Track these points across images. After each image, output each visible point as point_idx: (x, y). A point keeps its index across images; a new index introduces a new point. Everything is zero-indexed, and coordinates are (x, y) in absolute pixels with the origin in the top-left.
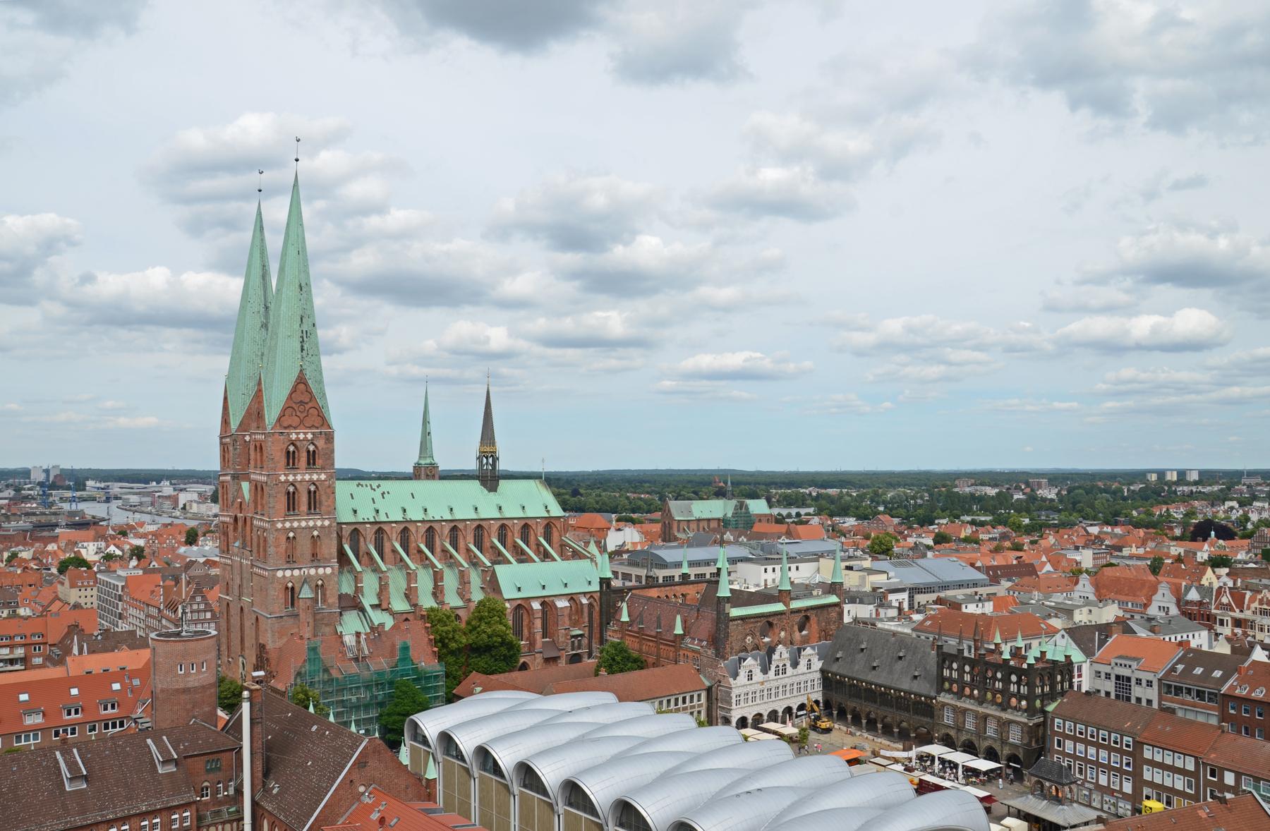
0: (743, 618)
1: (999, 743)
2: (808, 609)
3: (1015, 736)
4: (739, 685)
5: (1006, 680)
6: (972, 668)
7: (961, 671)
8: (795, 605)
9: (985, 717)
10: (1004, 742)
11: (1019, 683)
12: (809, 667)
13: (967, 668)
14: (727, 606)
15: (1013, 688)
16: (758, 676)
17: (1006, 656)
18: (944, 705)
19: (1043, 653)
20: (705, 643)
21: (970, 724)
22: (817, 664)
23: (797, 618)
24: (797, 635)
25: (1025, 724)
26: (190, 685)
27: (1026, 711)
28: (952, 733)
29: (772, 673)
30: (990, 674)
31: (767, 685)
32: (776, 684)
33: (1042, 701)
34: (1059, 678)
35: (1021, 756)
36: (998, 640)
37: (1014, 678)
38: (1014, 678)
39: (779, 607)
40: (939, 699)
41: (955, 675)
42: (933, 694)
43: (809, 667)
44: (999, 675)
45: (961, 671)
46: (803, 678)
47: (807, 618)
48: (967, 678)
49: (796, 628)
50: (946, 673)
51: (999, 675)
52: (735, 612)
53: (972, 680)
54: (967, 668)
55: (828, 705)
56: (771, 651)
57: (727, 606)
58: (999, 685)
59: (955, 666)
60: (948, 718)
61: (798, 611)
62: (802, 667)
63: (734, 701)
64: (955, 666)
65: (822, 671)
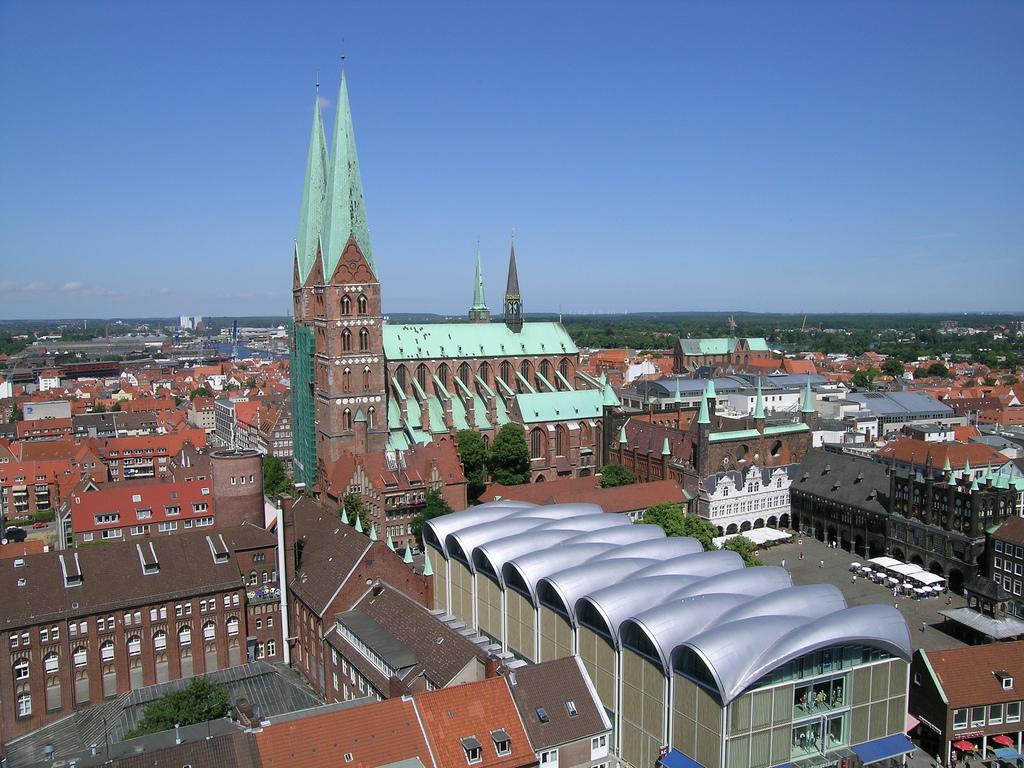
0: (719, 442)
2: (780, 435)
4: (716, 498)
8: (769, 431)
12: (779, 485)
14: (707, 431)
16: (733, 492)
17: (953, 482)
22: (787, 483)
23: (771, 443)
24: (770, 456)
26: (241, 494)
28: (902, 548)
29: (745, 489)
31: (741, 500)
32: (749, 499)
33: (984, 524)
34: (1002, 504)
36: (948, 467)
39: (754, 433)
43: (779, 485)
47: (779, 444)
52: (713, 437)
55: (794, 516)
56: (746, 470)
57: (707, 431)
61: (771, 436)
62: (773, 486)
63: (711, 510)
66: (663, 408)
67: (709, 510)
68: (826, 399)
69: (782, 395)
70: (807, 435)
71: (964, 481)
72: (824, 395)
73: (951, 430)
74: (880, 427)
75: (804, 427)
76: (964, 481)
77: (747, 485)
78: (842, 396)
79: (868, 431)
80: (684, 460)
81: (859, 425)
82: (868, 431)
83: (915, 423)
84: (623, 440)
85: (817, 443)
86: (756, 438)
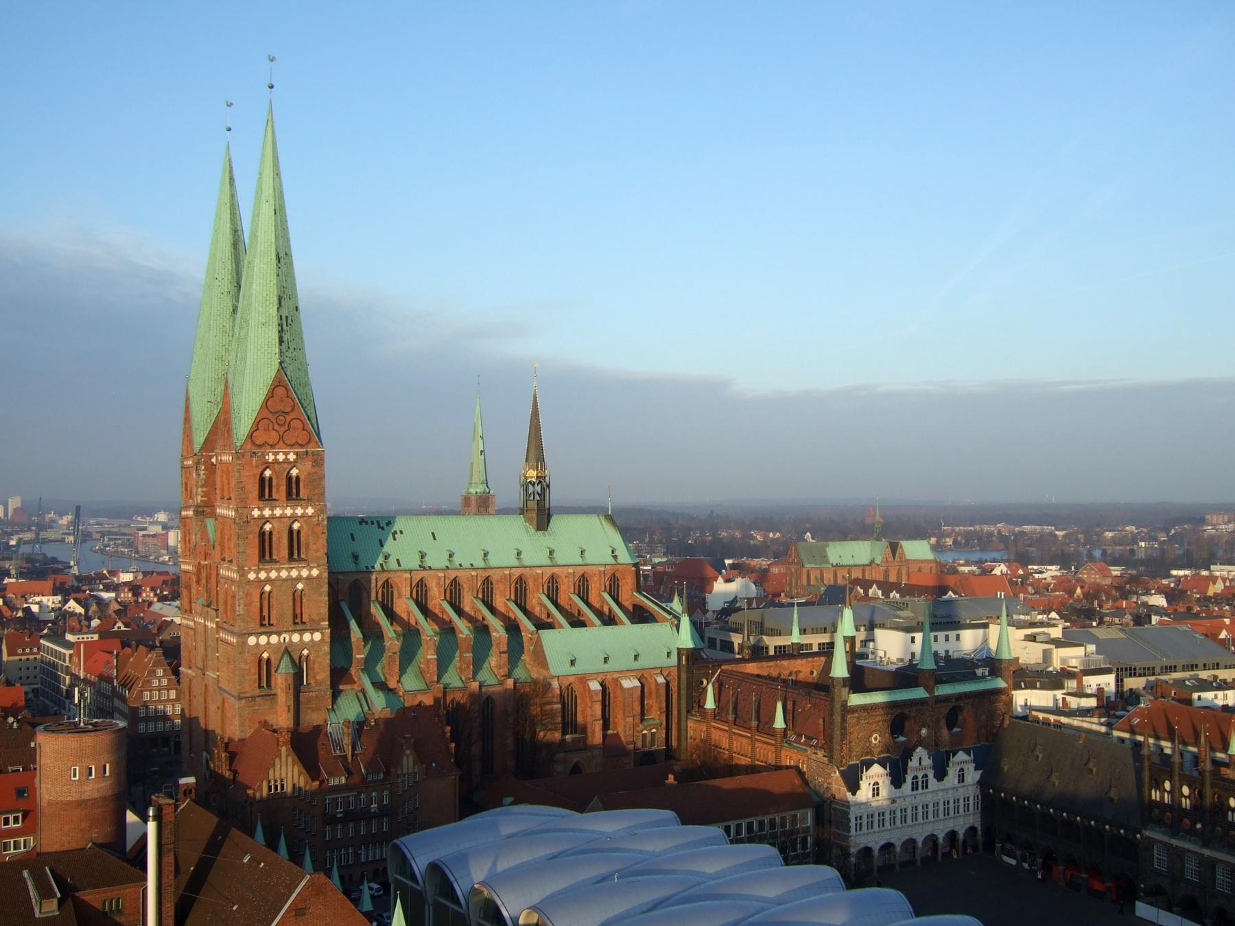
8: (944, 690)
12: (961, 778)
18: (1153, 841)
20: (814, 742)
21: (1190, 869)
22: (972, 776)
24: (945, 732)
29: (907, 786)
39: (919, 693)
40: (1147, 833)
43: (961, 778)
46: (950, 796)
49: (943, 723)
52: (856, 700)
55: (988, 831)
56: (907, 754)
59: (1167, 785)
60: (1159, 861)
63: (853, 824)
64: (1167, 785)
65: (981, 783)
66: (772, 652)
67: (849, 821)
68: (1032, 638)
72: (1029, 631)
74: (1119, 681)
77: (909, 778)
78: (1056, 632)
80: (809, 738)
83: (1176, 675)
84: (710, 704)
86: (921, 702)
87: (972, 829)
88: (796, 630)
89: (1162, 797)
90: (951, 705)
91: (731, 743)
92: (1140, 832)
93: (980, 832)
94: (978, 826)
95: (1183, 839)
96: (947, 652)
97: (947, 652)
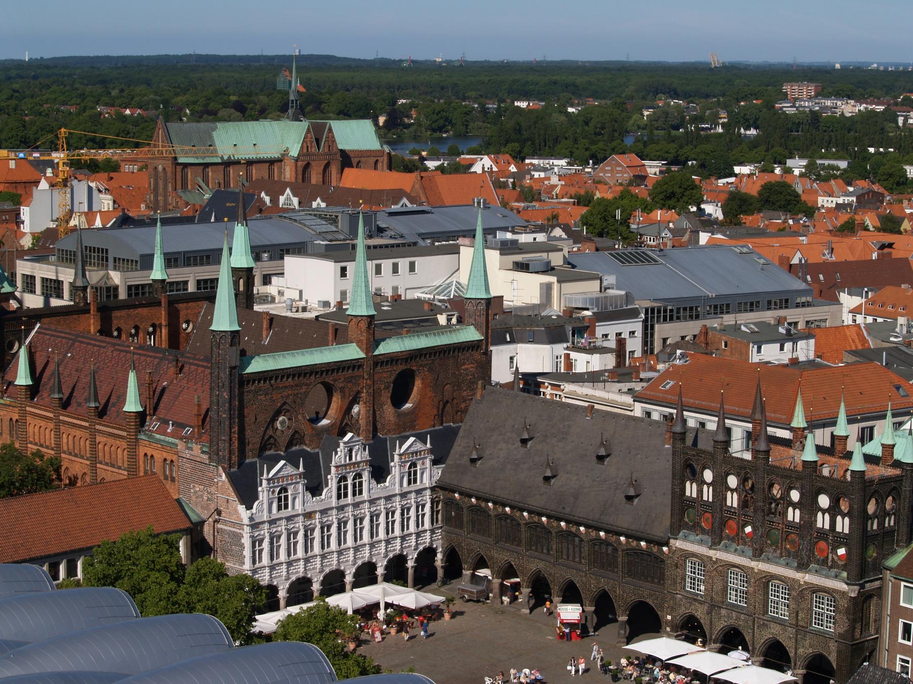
1: (791, 631)
3: (827, 622)
5: (809, 506)
6: (743, 481)
7: (720, 485)
9: (766, 580)
10: (801, 630)
11: (834, 510)
13: (732, 481)
15: (822, 521)
17: (810, 455)
19: (889, 449)
23: (388, 375)
24: (388, 410)
25: (844, 593)
27: (845, 568)
28: (700, 613)
30: (776, 491)
35: (833, 658)
36: (799, 421)
37: (824, 501)
38: (824, 501)
40: (678, 544)
41: (708, 494)
42: (659, 530)
44: (795, 496)
45: (720, 485)
48: (732, 500)
50: (691, 490)
51: (795, 496)
53: (744, 504)
54: (732, 481)
55: (452, 556)
58: (794, 515)
59: (708, 475)
61: (392, 359)
64: (708, 475)
69: (419, 261)
70: (477, 355)
71: (835, 449)
72: (519, 258)
73: (807, 337)
75: (471, 334)
76: (835, 449)
79: (621, 343)
80: (179, 425)
81: (607, 331)
82: (621, 343)
83: (729, 319)
84: (23, 378)
85: (501, 373)
87: (428, 554)
88: (158, 261)
89: (700, 492)
90: (401, 367)
91: (58, 436)
92: (667, 544)
93: (439, 556)
94: (439, 546)
95: (726, 549)
96: (395, 289)
97: (395, 289)
